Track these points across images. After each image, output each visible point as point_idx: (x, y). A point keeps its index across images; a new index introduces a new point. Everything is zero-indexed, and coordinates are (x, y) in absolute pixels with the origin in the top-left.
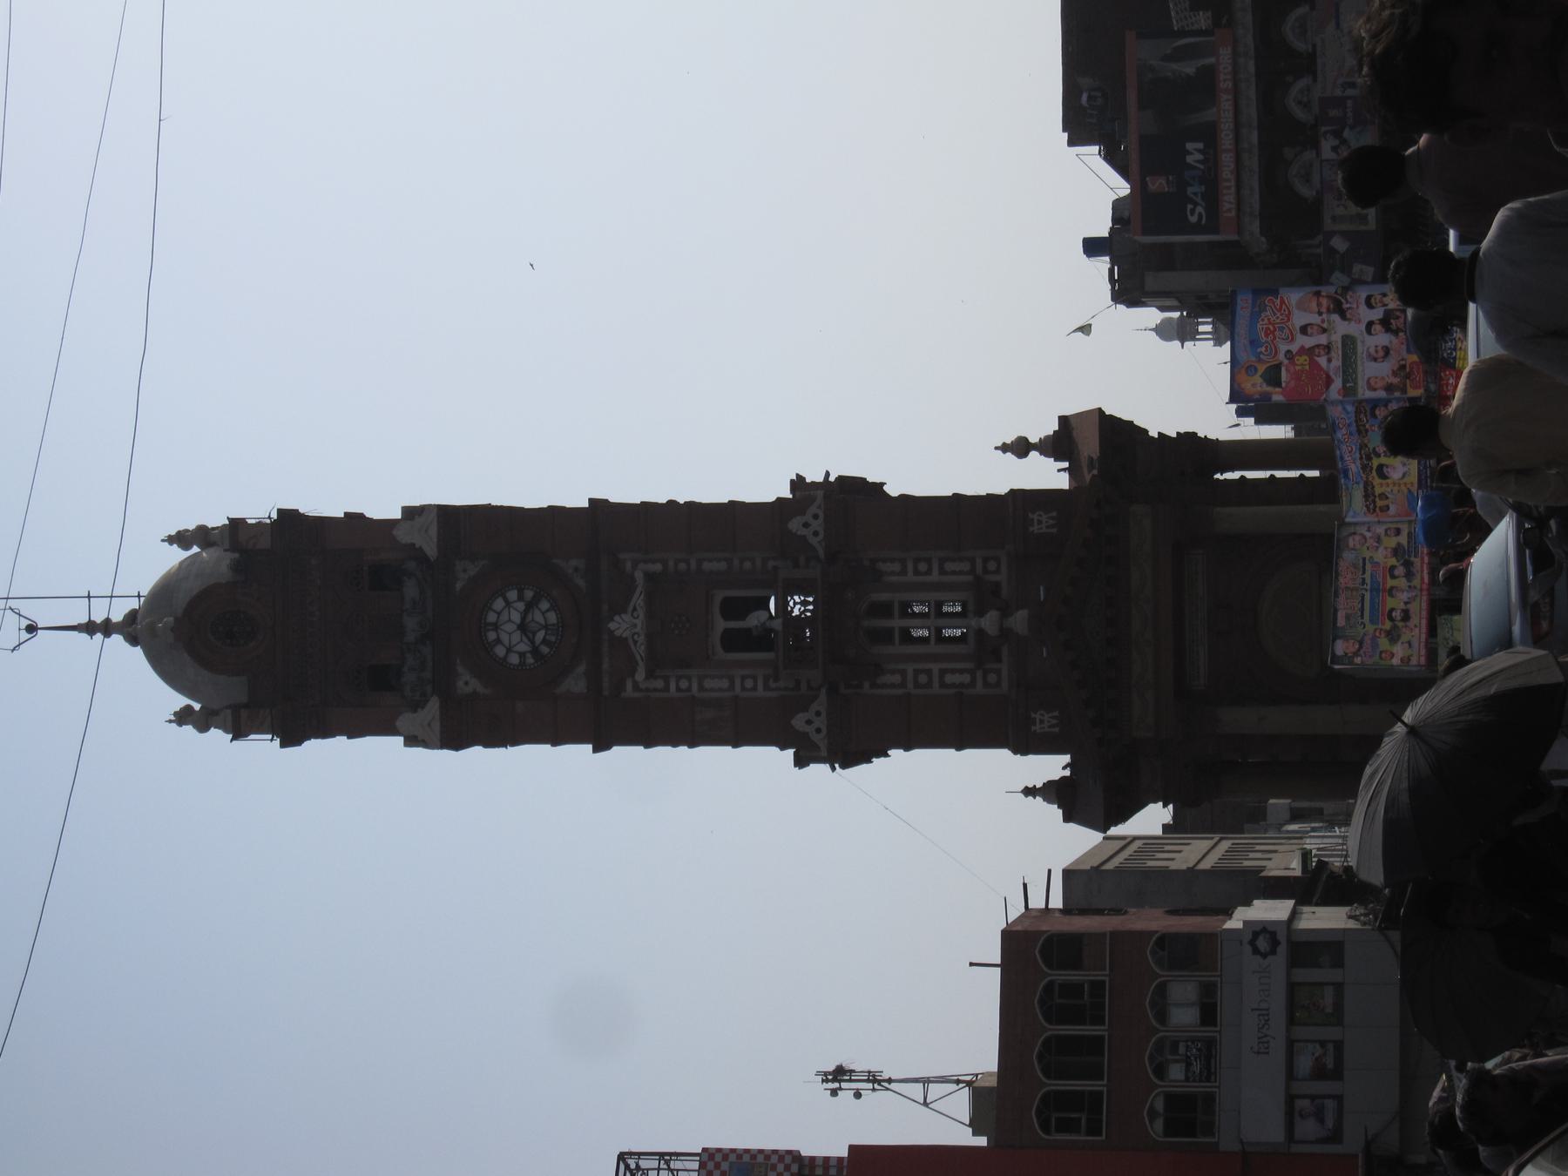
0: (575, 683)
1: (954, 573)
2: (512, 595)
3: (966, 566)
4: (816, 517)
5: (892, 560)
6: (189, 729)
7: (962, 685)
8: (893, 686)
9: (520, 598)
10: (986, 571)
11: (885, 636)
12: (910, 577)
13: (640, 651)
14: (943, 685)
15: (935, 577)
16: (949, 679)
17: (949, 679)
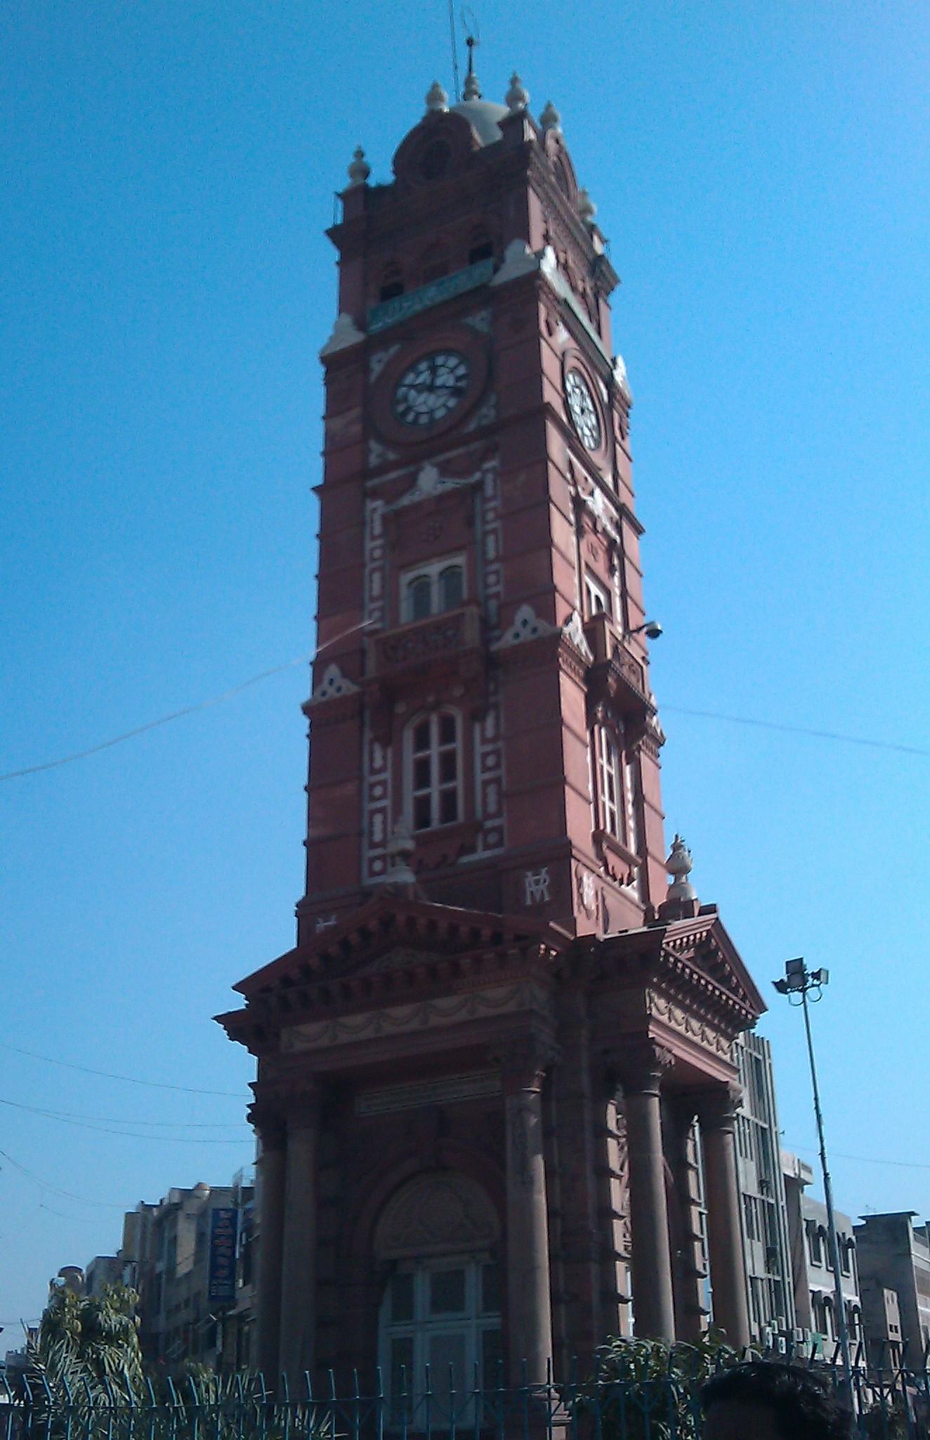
0: (376, 453)
1: (485, 796)
2: (461, 371)
3: (492, 808)
4: (535, 630)
5: (497, 726)
6: (352, 160)
7: (371, 833)
8: (372, 760)
9: (458, 379)
10: (487, 832)
11: (422, 741)
12: (479, 749)
13: (406, 501)
14: (373, 812)
15: (480, 777)
16: (378, 819)
17: (378, 819)
